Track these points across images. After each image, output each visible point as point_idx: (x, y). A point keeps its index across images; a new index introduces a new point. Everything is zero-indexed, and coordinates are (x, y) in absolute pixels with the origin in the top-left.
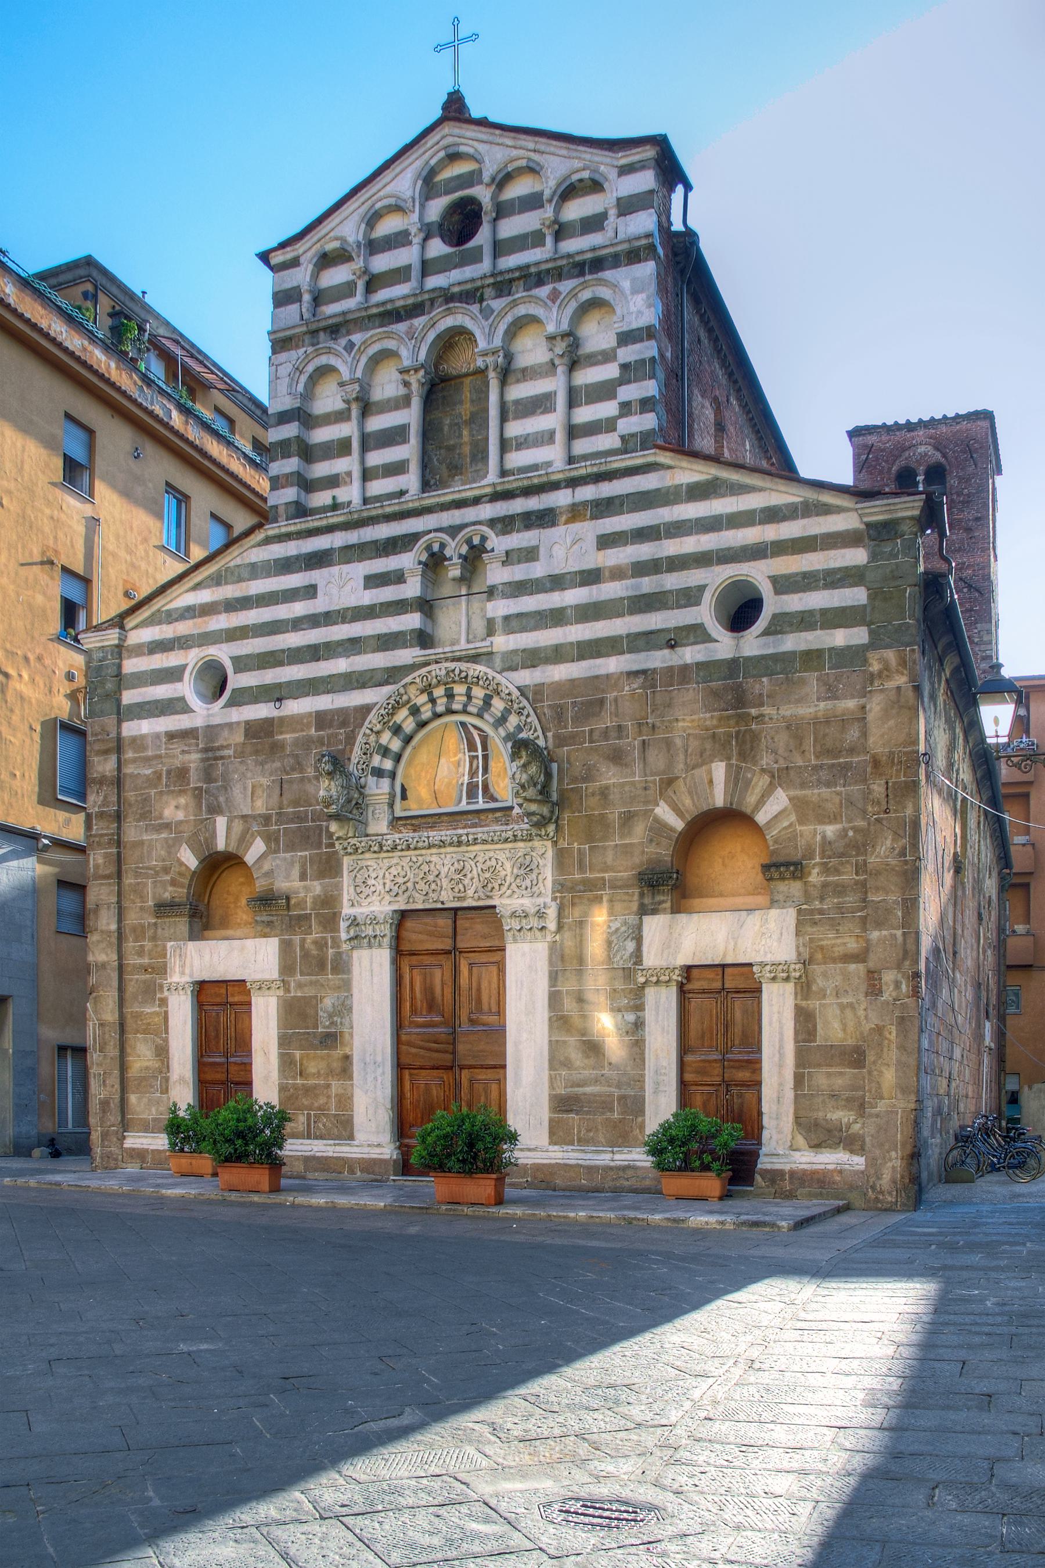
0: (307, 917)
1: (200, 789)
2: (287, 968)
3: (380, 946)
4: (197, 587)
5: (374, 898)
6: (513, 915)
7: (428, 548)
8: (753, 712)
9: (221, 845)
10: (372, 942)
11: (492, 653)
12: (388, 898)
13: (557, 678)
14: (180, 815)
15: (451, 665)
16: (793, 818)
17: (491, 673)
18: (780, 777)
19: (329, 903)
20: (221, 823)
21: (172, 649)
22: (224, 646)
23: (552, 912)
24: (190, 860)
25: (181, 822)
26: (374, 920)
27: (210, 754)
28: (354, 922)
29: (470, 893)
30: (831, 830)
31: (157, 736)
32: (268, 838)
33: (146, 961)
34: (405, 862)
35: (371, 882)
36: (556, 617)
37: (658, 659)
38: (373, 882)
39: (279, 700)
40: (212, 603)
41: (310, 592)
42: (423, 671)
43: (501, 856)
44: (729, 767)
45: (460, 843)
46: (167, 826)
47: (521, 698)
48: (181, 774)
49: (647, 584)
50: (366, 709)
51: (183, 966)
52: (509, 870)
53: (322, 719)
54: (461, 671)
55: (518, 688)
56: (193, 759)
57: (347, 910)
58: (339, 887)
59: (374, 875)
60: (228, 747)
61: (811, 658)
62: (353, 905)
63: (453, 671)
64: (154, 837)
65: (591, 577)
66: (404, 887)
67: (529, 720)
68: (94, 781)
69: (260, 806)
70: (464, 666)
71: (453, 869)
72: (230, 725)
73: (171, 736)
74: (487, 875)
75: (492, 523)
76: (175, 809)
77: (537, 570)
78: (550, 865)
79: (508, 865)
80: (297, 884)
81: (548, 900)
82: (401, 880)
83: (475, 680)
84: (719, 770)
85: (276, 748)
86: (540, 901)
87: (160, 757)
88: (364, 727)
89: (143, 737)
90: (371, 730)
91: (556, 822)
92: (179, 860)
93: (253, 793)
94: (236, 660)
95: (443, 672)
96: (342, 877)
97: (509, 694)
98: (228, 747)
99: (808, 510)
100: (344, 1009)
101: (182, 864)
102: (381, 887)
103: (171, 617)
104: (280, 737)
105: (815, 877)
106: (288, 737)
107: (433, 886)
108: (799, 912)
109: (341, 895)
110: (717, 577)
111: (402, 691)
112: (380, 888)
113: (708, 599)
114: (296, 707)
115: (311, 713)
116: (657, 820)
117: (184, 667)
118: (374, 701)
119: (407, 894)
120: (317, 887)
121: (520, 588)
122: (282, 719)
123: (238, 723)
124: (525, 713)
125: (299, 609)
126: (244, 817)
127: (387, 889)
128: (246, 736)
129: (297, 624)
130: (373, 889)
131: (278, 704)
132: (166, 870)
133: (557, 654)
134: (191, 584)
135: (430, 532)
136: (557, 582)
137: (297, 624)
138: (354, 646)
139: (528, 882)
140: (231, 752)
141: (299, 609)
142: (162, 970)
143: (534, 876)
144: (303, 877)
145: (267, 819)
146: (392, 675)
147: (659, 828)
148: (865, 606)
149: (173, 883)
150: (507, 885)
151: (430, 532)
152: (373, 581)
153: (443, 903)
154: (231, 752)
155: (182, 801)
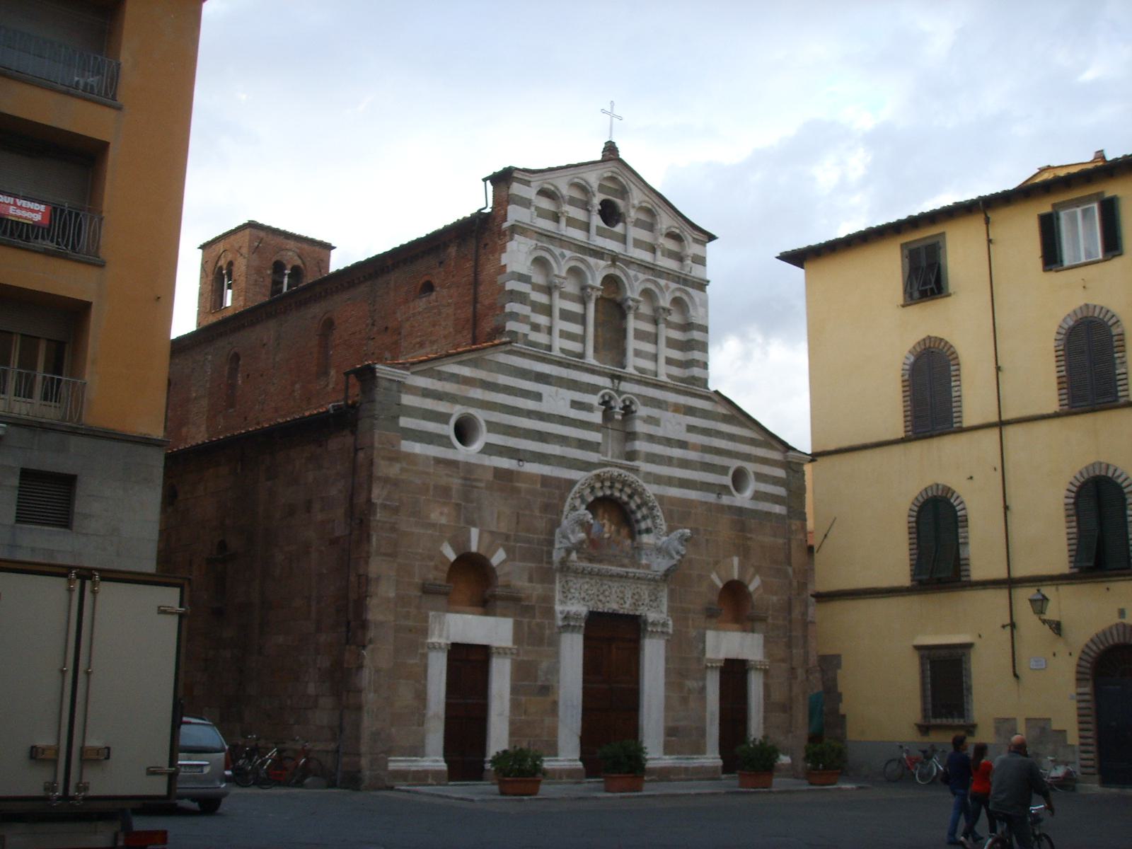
0: (533, 607)
1: (458, 505)
2: (517, 638)
3: (578, 632)
4: (460, 363)
6: (654, 624)
7: (603, 396)
8: (749, 535)
9: (474, 548)
10: (574, 629)
11: (637, 470)
12: (582, 602)
13: (670, 494)
14: (443, 520)
15: (622, 471)
16: (761, 591)
17: (641, 482)
18: (758, 570)
19: (548, 600)
20: (474, 532)
21: (441, 400)
22: (479, 411)
23: (670, 623)
24: (452, 556)
25: (444, 525)
26: (576, 616)
27: (468, 482)
28: (567, 617)
29: (627, 606)
30: (775, 598)
31: (427, 457)
32: (507, 551)
33: (410, 623)
34: (593, 582)
35: (572, 591)
36: (669, 461)
37: (711, 498)
39: (520, 460)
40: (472, 378)
41: (538, 397)
42: (608, 469)
43: (644, 587)
44: (740, 560)
45: (626, 577)
46: (433, 525)
48: (445, 491)
49: (708, 458)
50: (572, 483)
51: (441, 630)
52: (646, 596)
53: (545, 480)
54: (625, 476)
55: (655, 495)
56: (456, 482)
57: (558, 608)
58: (553, 590)
60: (480, 481)
61: (768, 514)
63: (620, 475)
64: (422, 531)
65: (683, 445)
68: (379, 478)
69: (503, 527)
70: (627, 473)
71: (618, 591)
72: (483, 467)
73: (439, 461)
74: (636, 597)
75: (638, 396)
76: (439, 515)
77: (659, 432)
78: (666, 596)
79: (647, 593)
80: (527, 584)
81: (664, 616)
84: (736, 560)
85: (516, 491)
87: (428, 474)
88: (571, 495)
89: (415, 455)
92: (441, 552)
93: (498, 517)
94: (488, 423)
95: (616, 474)
98: (480, 481)
99: (752, 442)
100: (555, 670)
101: (444, 557)
103: (441, 376)
104: (517, 484)
105: (770, 620)
106: (522, 485)
108: (765, 637)
109: (553, 597)
110: (735, 464)
113: (731, 473)
114: (532, 468)
116: (712, 581)
117: (448, 416)
120: (537, 589)
121: (651, 438)
122: (518, 473)
123: (490, 467)
125: (530, 404)
126: (492, 533)
127: (582, 596)
128: (495, 477)
129: (530, 414)
131: (521, 463)
132: (431, 558)
133: (670, 481)
134: (459, 360)
135: (606, 388)
136: (668, 442)
137: (530, 414)
138: (563, 440)
139: (655, 604)
140: (482, 485)
141: (530, 404)
142: (425, 632)
144: (530, 580)
145: (507, 537)
146: (587, 466)
147: (713, 585)
148: (785, 498)
149: (436, 568)
151: (606, 388)
152: (576, 405)
154: (482, 485)
155: (446, 510)
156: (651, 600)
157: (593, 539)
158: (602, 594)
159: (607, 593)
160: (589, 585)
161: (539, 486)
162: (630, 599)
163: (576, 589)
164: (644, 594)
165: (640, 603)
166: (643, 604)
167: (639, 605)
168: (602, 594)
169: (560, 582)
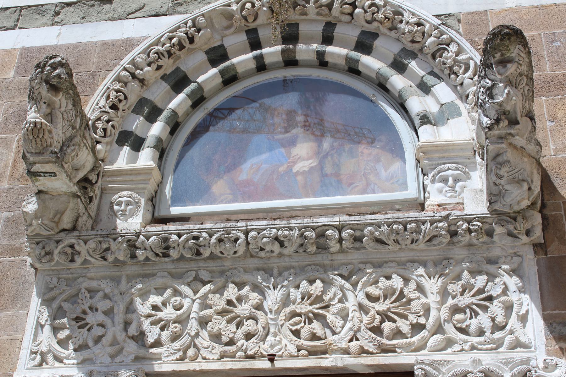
5: (97, 349)
29: (340, 340)
35: (91, 319)
38: (100, 317)
47: (443, 28)
52: (433, 299)
59: (103, 305)
62: (43, 361)
66: (174, 328)
67: (461, 57)
74: (382, 306)
82: (168, 313)
83: (347, 9)
86: (519, 354)
88: (117, 70)
90: (133, 76)
91: (540, 211)
96: (26, 306)
97: (419, 24)
102: (119, 327)
107: (249, 325)
111: (202, 20)
112: (115, 330)
115: (14, 50)
118: (143, 34)
119: (177, 345)
124: (453, 48)
130: (98, 331)
139: (483, 320)
143: (496, 308)
150: (430, 323)
153: (272, 358)
156: (456, 310)
157: (247, 183)
158: (222, 313)
159: (243, 309)
160: (169, 292)
161: (12, 74)
162: (354, 315)
163: (109, 313)
164: (420, 288)
165: (404, 326)
166: (417, 328)
167: (398, 334)
168: (222, 313)
169: (47, 302)
